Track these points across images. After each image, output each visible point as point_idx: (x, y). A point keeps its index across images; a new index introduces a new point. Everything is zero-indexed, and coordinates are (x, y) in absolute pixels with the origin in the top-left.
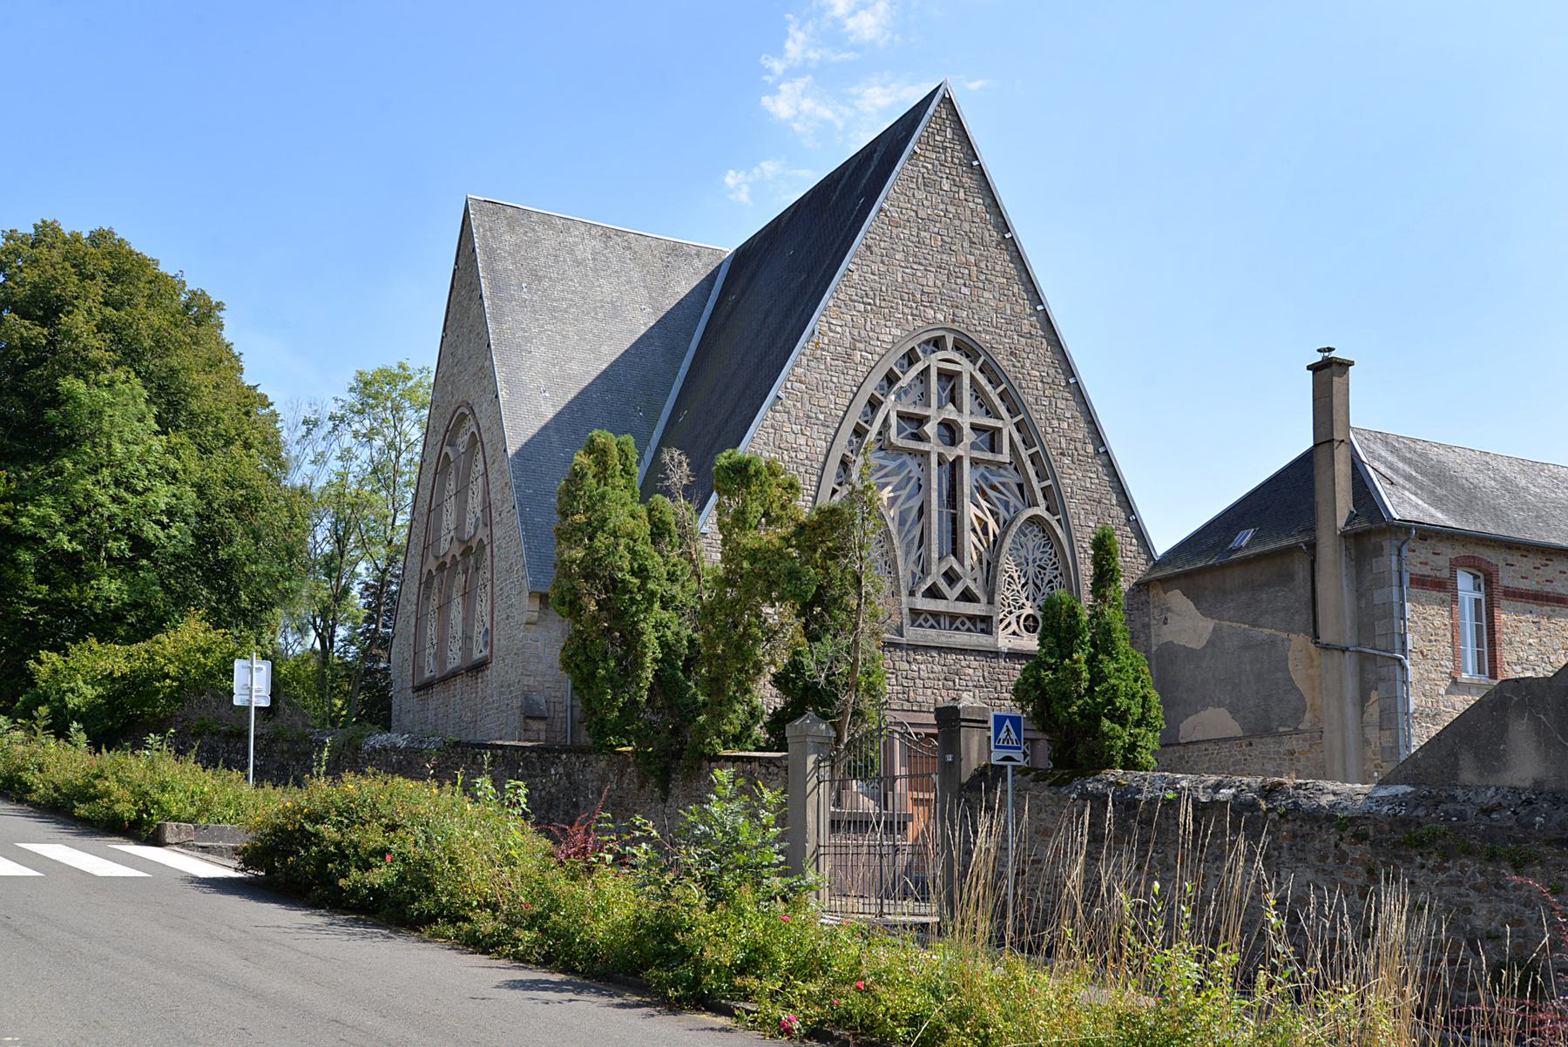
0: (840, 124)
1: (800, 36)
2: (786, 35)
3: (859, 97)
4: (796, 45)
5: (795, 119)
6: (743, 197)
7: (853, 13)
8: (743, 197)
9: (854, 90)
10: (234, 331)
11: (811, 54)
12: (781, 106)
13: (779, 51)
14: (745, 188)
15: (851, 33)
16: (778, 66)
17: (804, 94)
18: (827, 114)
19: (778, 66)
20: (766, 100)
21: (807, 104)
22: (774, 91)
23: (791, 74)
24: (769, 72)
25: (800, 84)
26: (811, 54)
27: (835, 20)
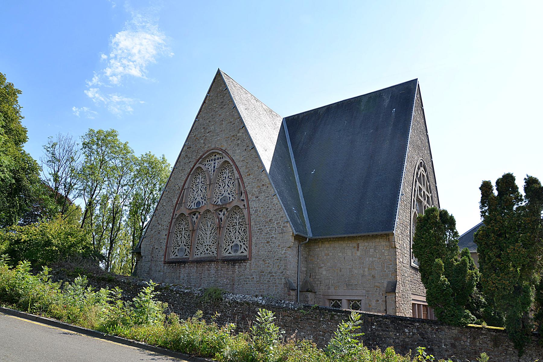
0: (106, 103)
1: (97, 78)
2: (93, 77)
3: (111, 97)
4: (95, 80)
5: (93, 98)
6: (77, 114)
7: (112, 76)
8: (77, 114)
9: (110, 95)
10: (21, 99)
11: (99, 83)
12: (90, 94)
13: (91, 80)
14: (78, 112)
15: (111, 81)
16: (90, 84)
17: (96, 92)
18: (103, 99)
19: (90, 84)
20: (85, 91)
21: (97, 95)
22: (88, 90)
23: (93, 86)
24: (88, 84)
25: (96, 90)
26: (99, 83)
27: (106, 76)
